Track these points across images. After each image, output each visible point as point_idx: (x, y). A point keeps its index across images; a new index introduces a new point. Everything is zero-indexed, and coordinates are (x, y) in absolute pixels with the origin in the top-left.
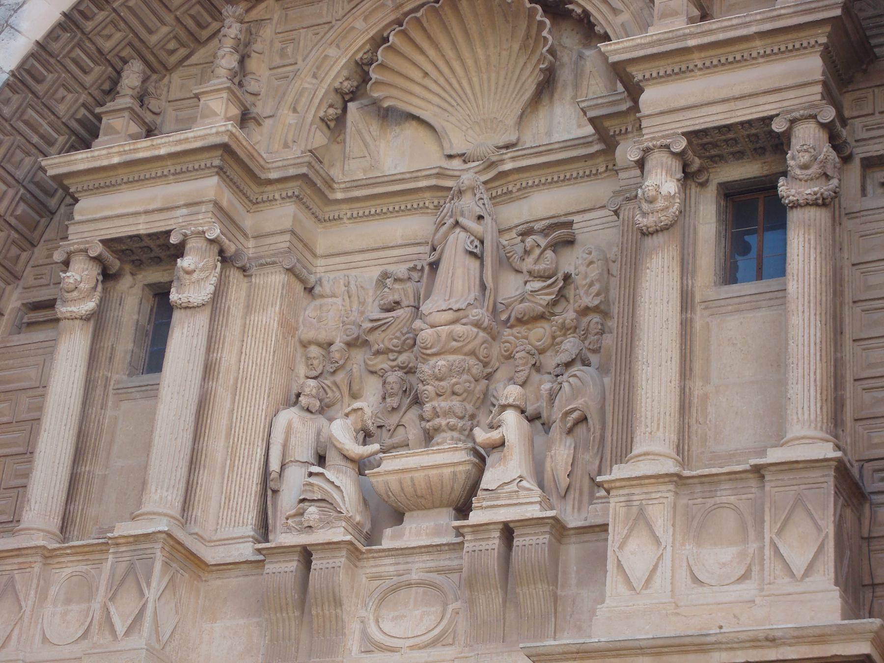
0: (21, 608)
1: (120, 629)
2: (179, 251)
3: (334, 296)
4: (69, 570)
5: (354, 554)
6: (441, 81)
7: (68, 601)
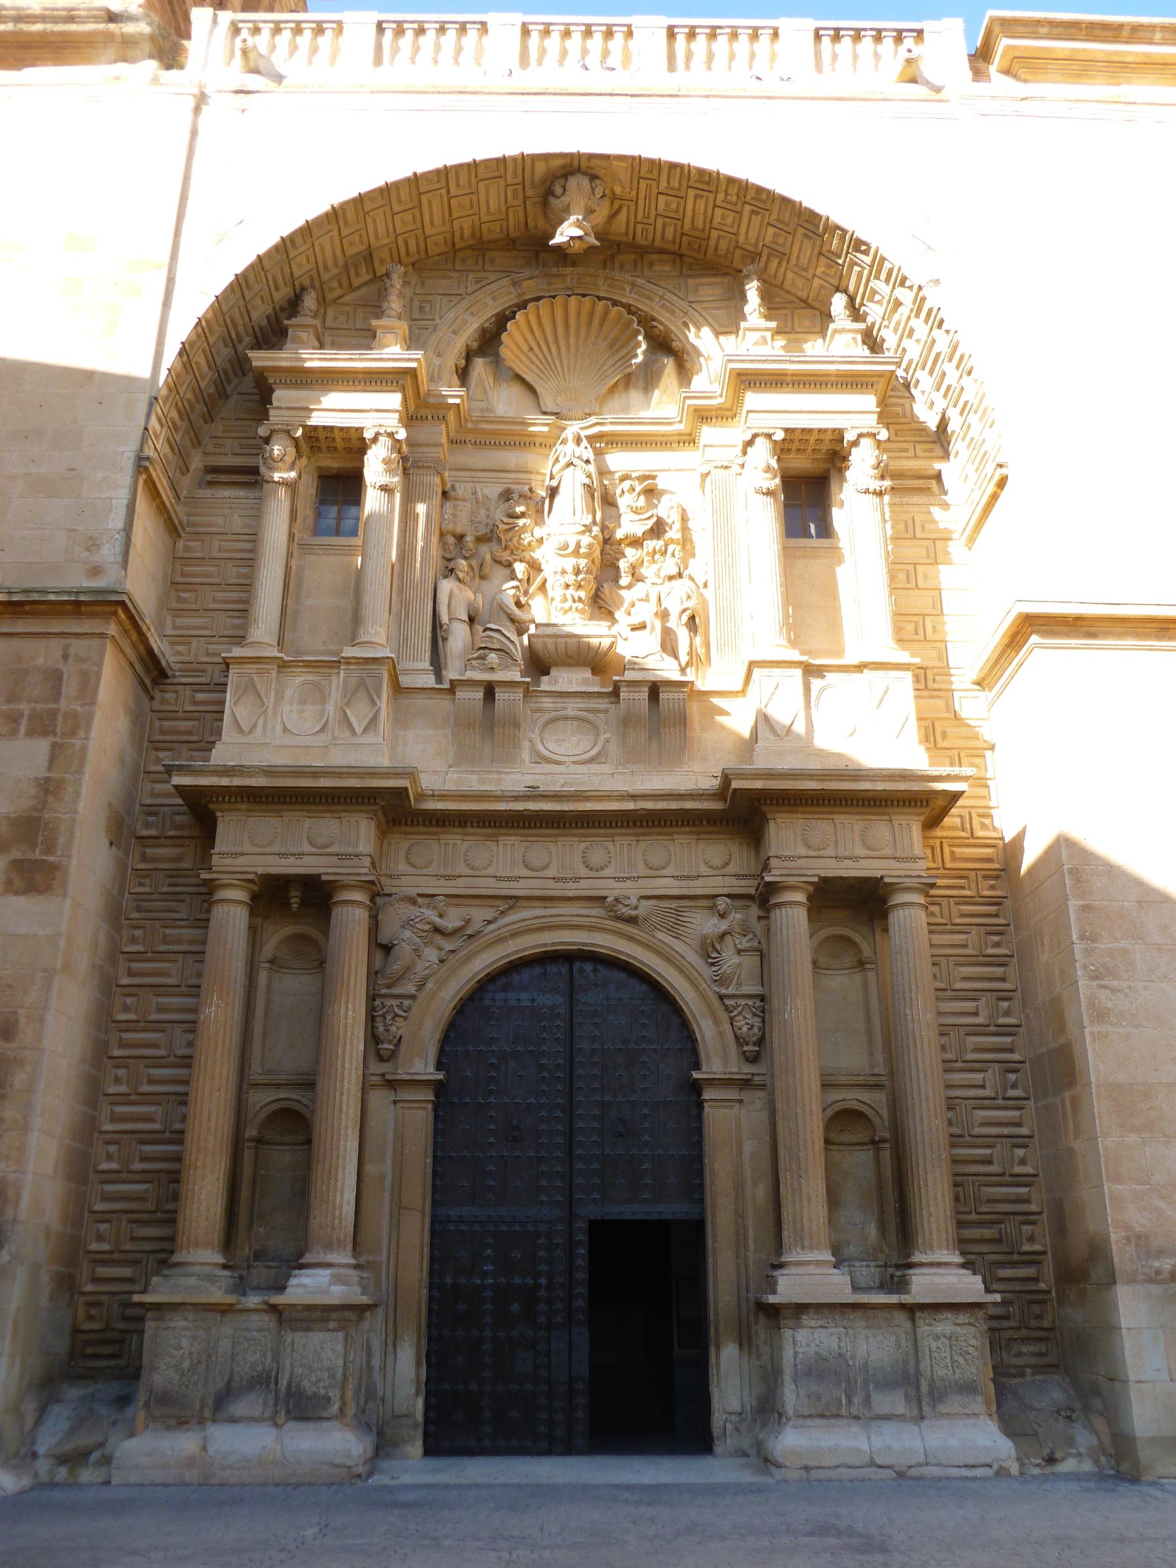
0: (263, 704)
1: (359, 729)
3: (464, 500)
4: (302, 679)
5: (527, 693)
6: (541, 356)
7: (303, 702)
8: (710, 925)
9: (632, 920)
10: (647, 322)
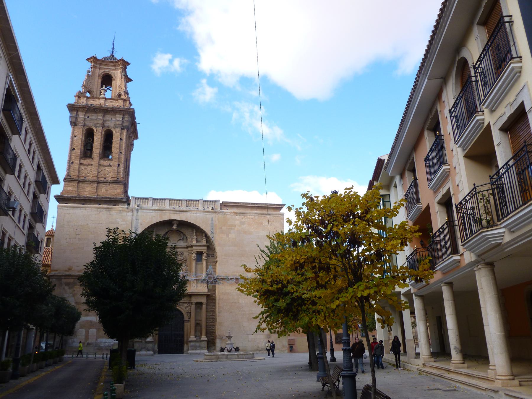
8: (186, 305)
10: (183, 233)
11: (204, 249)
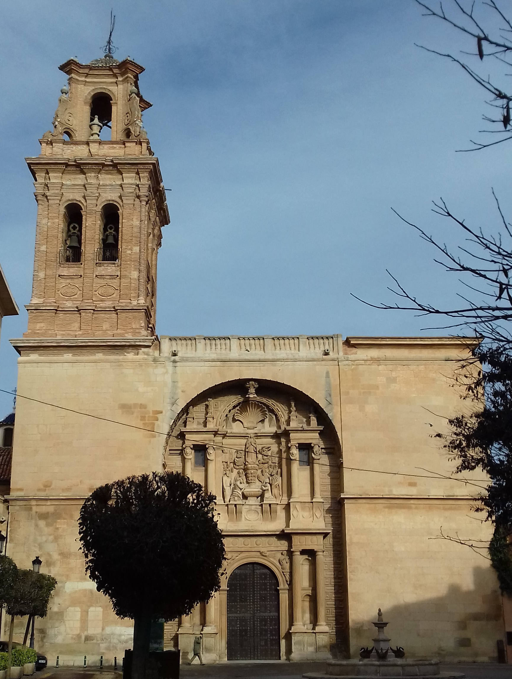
2: (207, 448)
9: (265, 556)
11: (313, 438)
